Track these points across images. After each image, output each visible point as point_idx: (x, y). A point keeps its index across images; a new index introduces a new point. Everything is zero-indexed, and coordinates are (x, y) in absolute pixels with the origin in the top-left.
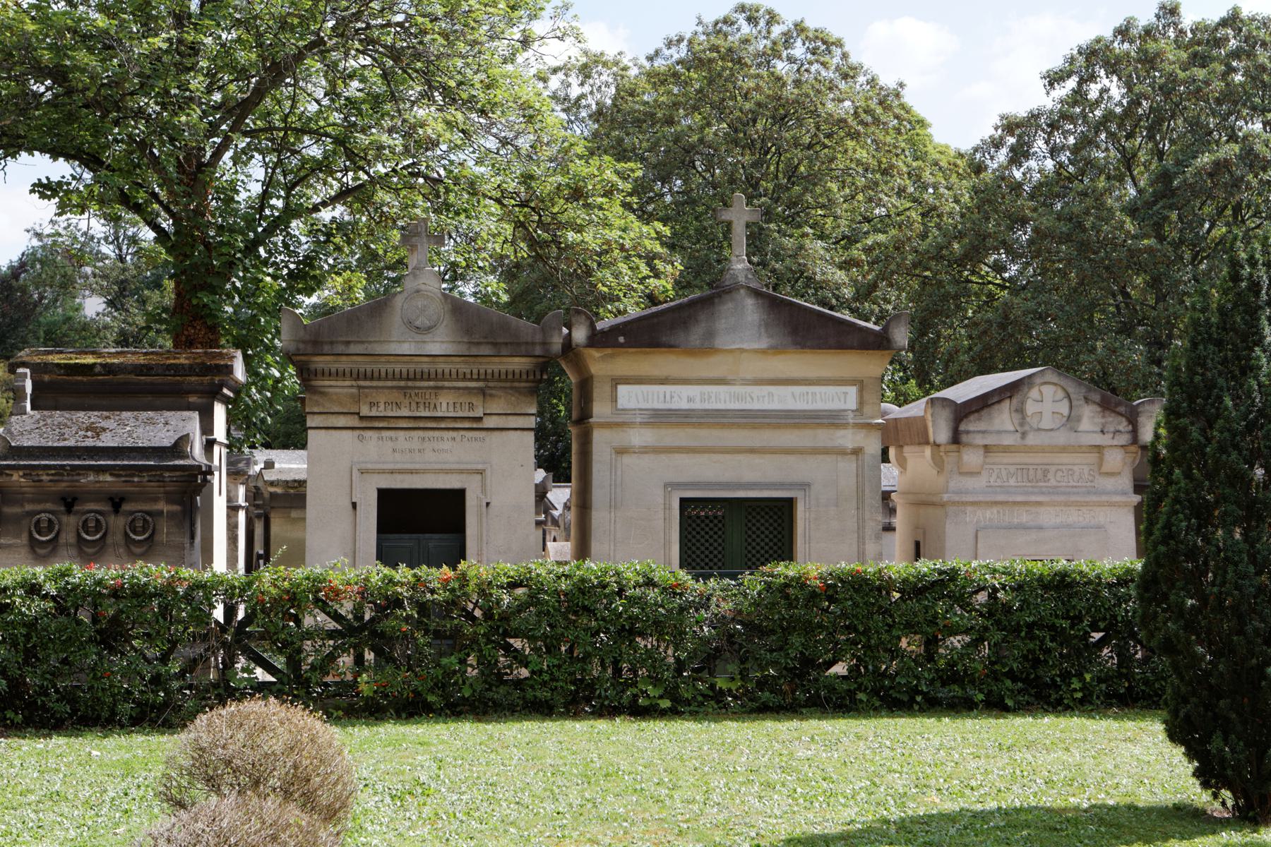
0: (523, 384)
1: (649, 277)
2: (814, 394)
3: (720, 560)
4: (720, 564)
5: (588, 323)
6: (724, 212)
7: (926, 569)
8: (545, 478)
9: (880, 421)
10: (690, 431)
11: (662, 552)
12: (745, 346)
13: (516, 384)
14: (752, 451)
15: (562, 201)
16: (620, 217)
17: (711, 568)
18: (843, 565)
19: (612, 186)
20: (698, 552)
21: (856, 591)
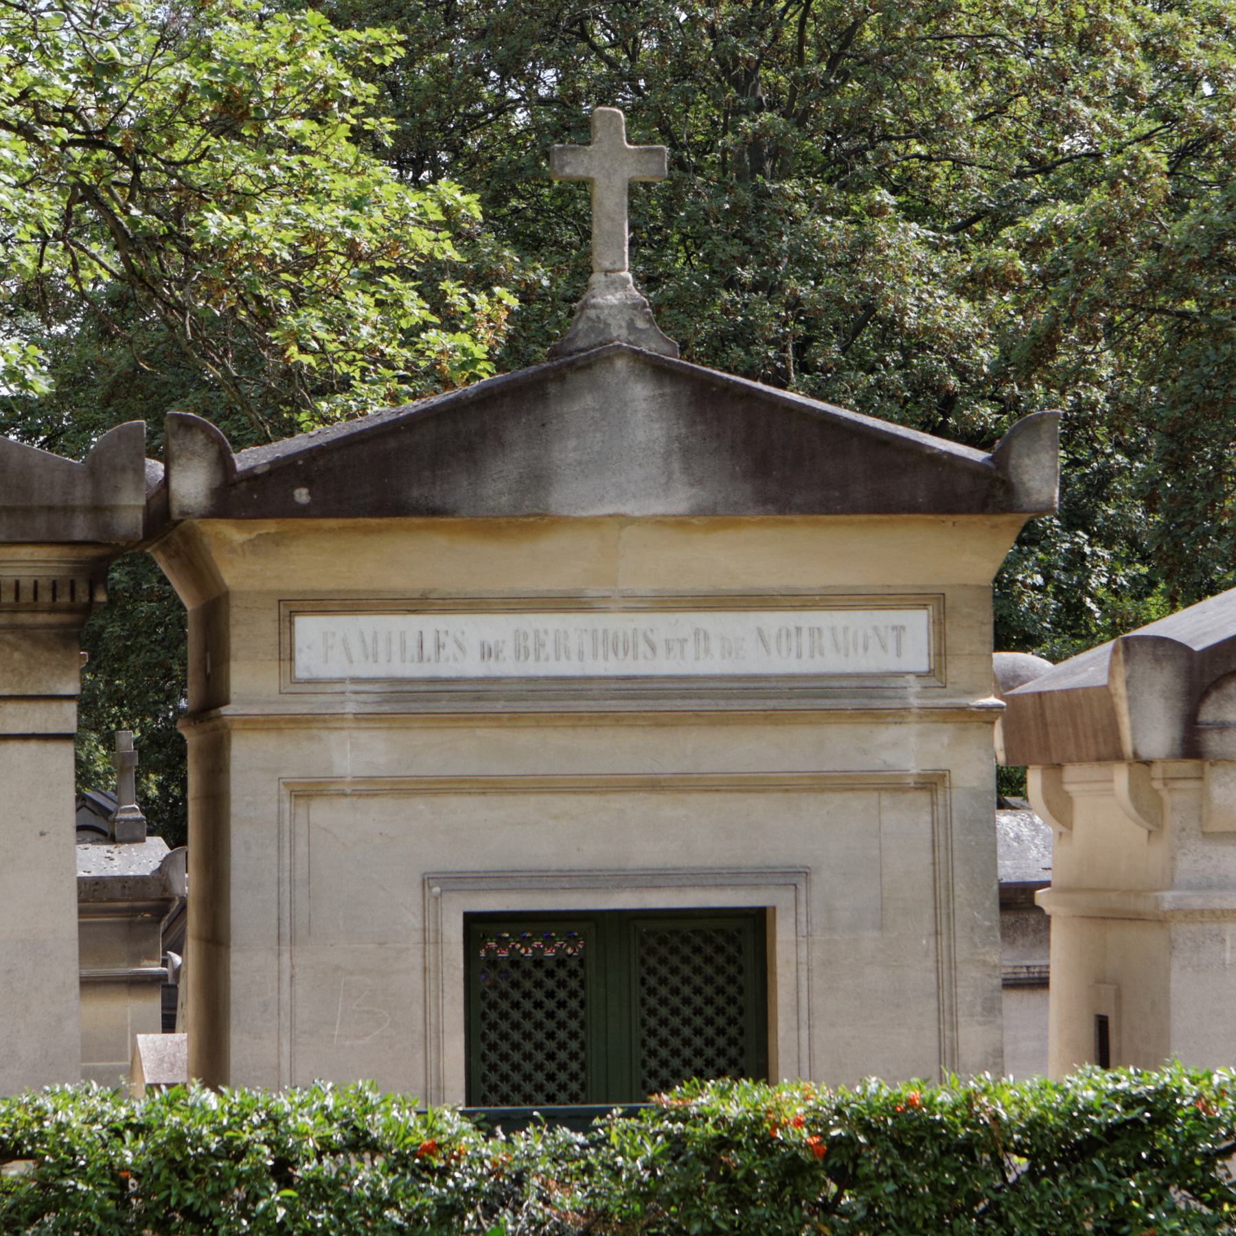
0: (42, 618)
1: (426, 326)
2: (816, 632)
3: (574, 1077)
4: (574, 1087)
5: (212, 453)
6: (569, 157)
7: (1091, 1094)
8: (166, 861)
9: (992, 700)
10: (488, 734)
11: (420, 1055)
12: (630, 508)
13: (25, 618)
14: (654, 785)
15: (196, 131)
16: (348, 172)
17: (528, 1099)
18: (873, 1086)
19: (326, 89)
20: (675, 1021)
21: (908, 1154)
